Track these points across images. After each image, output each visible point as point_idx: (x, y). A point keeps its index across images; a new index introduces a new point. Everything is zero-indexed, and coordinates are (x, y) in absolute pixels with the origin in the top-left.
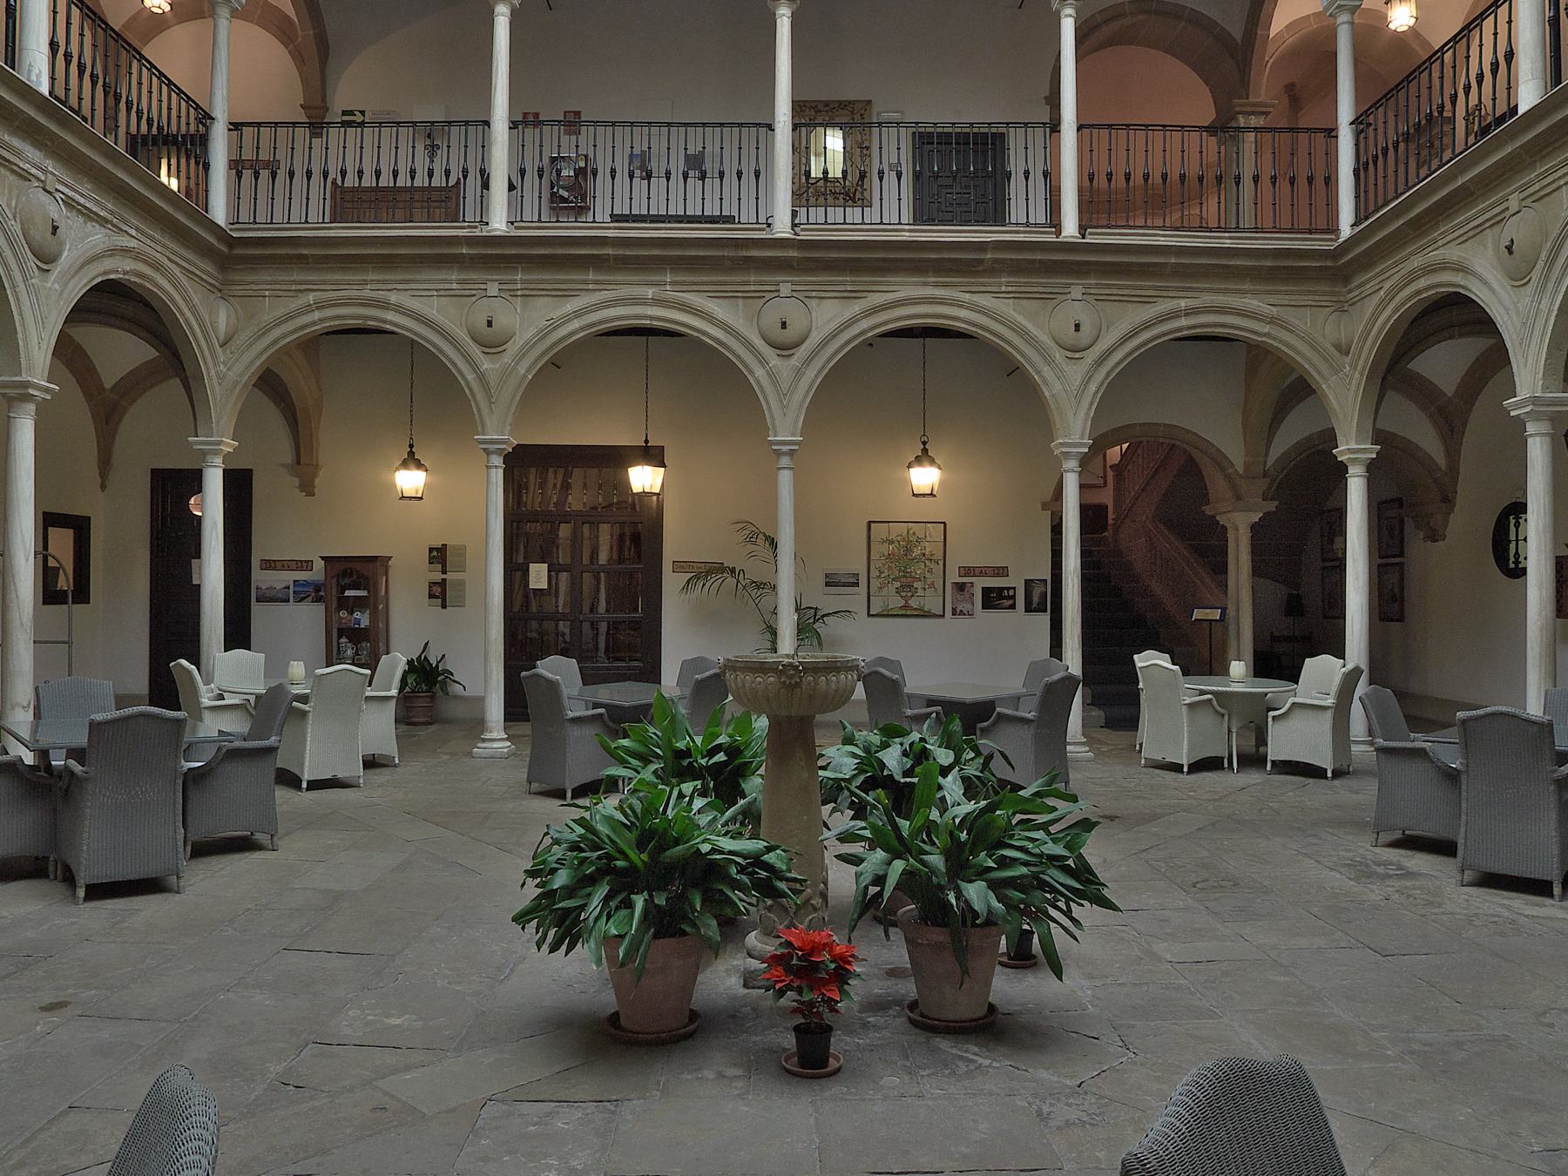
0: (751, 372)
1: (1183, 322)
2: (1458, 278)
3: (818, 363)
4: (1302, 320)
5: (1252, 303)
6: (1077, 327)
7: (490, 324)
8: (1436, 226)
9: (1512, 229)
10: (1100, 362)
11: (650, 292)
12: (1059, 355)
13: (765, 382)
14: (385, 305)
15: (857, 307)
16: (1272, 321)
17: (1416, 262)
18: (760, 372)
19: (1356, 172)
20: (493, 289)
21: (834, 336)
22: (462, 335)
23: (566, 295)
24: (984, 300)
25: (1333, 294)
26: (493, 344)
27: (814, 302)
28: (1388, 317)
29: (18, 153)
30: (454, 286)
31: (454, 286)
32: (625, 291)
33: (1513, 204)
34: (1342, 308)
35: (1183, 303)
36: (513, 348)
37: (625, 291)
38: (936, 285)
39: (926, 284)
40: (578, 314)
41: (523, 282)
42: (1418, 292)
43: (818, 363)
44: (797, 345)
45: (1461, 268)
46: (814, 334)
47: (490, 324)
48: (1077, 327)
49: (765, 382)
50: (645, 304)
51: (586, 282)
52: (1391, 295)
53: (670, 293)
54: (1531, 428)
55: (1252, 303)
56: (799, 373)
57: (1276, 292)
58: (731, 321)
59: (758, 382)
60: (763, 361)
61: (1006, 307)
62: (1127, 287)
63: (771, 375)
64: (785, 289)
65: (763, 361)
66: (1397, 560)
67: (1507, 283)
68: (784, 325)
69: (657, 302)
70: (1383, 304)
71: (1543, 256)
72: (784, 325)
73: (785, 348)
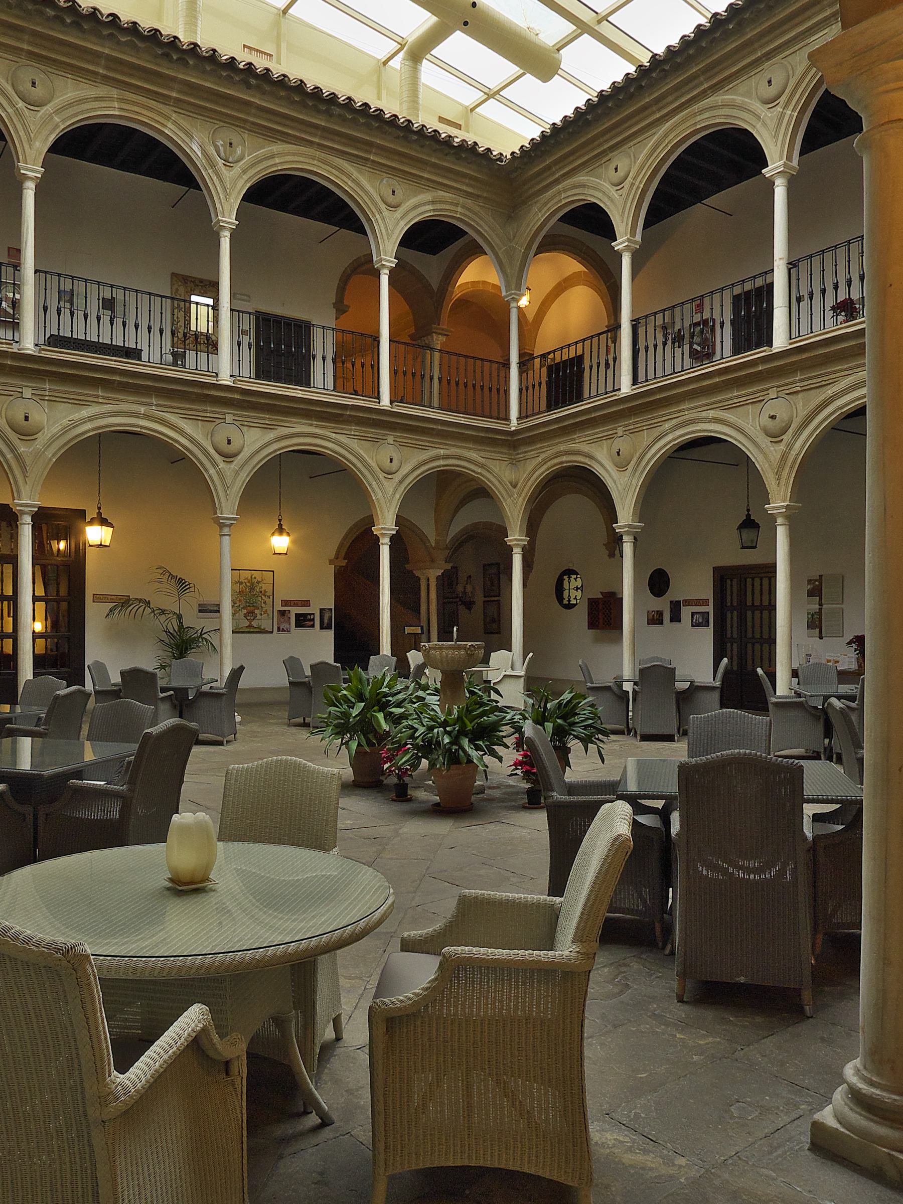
0: (207, 470)
1: (442, 462)
2: (587, 460)
3: (248, 468)
4: (495, 467)
5: (473, 455)
6: (391, 460)
7: (27, 419)
8: (574, 432)
9: (618, 444)
10: (401, 482)
11: (142, 410)
12: (381, 475)
13: (216, 478)
15: (272, 435)
16: (482, 466)
17: (562, 447)
18: (212, 471)
19: (520, 390)
20: (27, 393)
21: (258, 452)
23: (82, 404)
24: (343, 439)
25: (510, 454)
26: (27, 433)
27: (245, 429)
28: (542, 472)
32: (124, 407)
33: (620, 431)
34: (514, 463)
35: (442, 452)
37: (124, 407)
38: (317, 426)
39: (311, 425)
40: (90, 419)
41: (50, 390)
42: (562, 463)
43: (248, 468)
45: (592, 457)
46: (246, 449)
47: (27, 419)
48: (391, 460)
49: (216, 478)
52: (545, 461)
53: (154, 411)
54: (625, 538)
55: (473, 455)
56: (237, 473)
57: (485, 451)
58: (195, 435)
59: (210, 477)
60: (215, 464)
61: (354, 444)
62: (416, 440)
63: (220, 473)
64: (229, 418)
65: (215, 464)
66: (488, 599)
67: (615, 468)
68: (229, 442)
69: (147, 417)
70: (541, 465)
71: (635, 459)
72: (229, 442)
73: (229, 457)
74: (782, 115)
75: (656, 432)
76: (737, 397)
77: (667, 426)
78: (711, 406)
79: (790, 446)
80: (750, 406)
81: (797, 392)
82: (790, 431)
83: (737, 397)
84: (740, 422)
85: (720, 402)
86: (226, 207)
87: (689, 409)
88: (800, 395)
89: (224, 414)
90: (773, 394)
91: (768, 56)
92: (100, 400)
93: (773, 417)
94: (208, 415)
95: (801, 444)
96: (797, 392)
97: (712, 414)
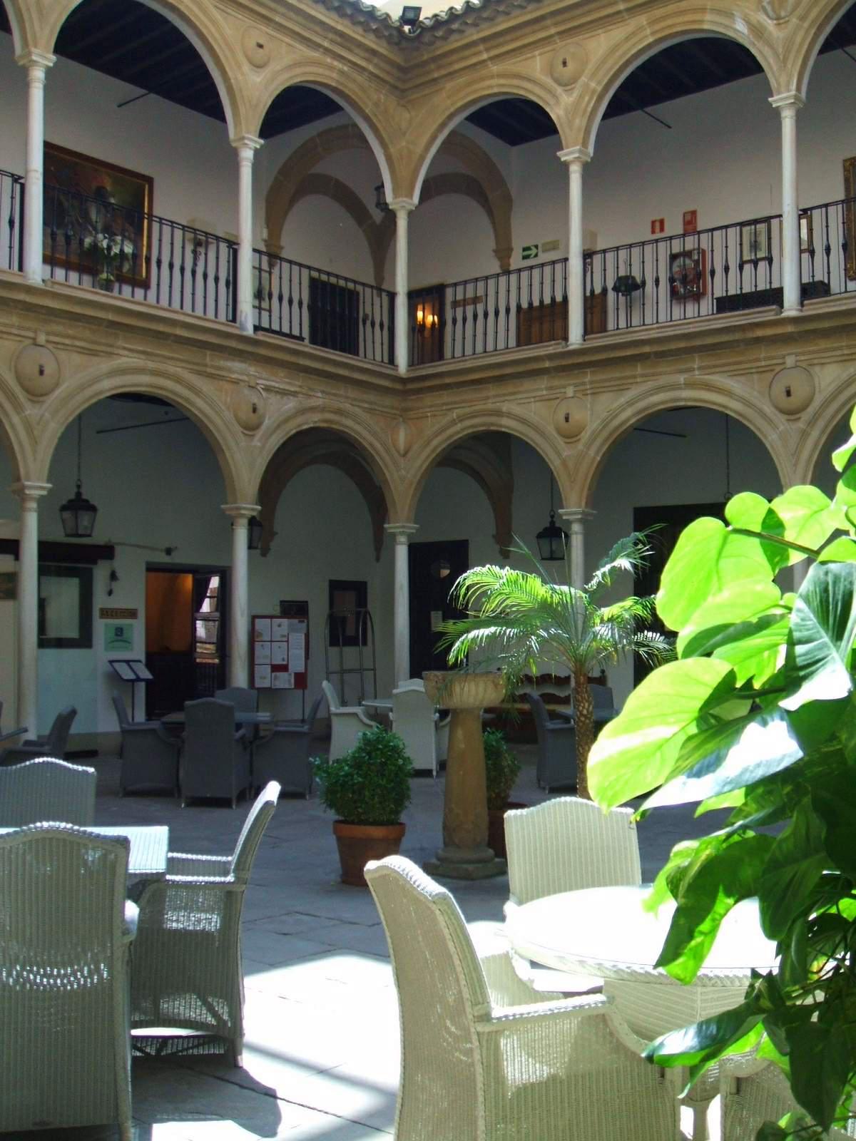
3: (821, 423)
11: (682, 378)
14: (499, 413)
20: (570, 391)
22: (551, 430)
23: (622, 389)
26: (571, 436)
27: (817, 369)
29: (230, 370)
30: (545, 392)
31: (545, 392)
32: (663, 380)
36: (585, 436)
37: (663, 380)
40: (630, 403)
41: (591, 382)
43: (821, 423)
44: (803, 408)
47: (567, 419)
50: (680, 389)
51: (635, 377)
53: (698, 375)
56: (804, 435)
64: (790, 361)
68: (788, 393)
69: (690, 385)
72: (788, 393)
86: (783, 80)
89: (784, 357)
92: (638, 380)
94: (763, 363)
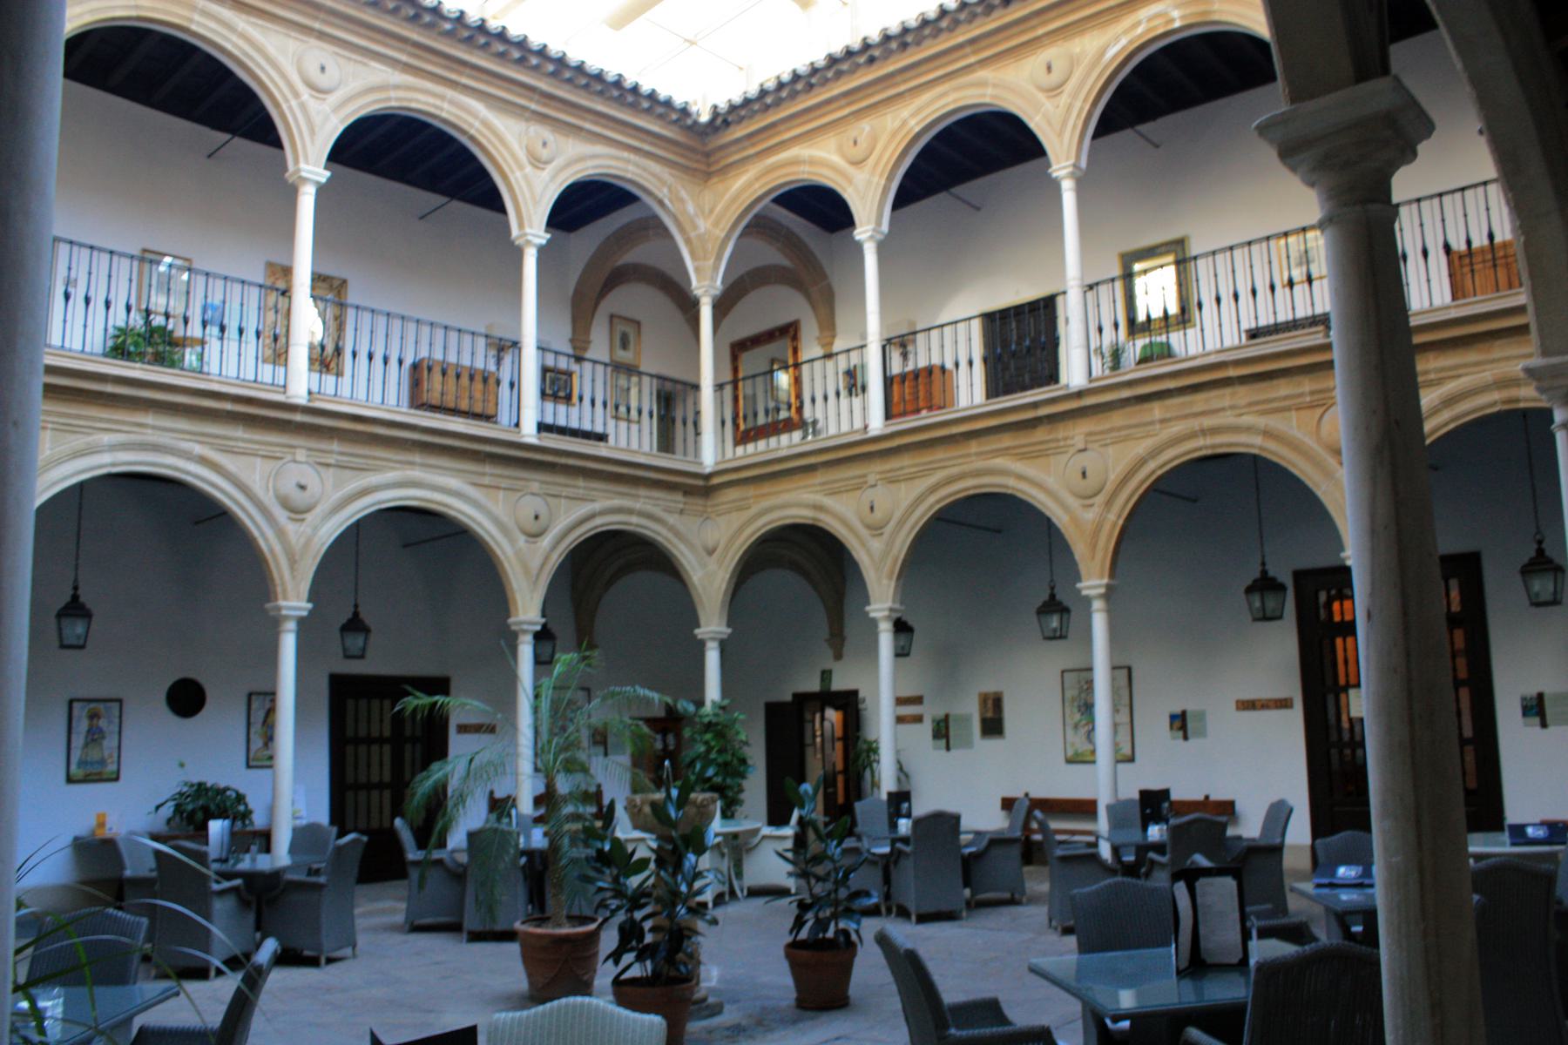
74: (326, 119)
75: (79, 441)
76: (244, 440)
77: (107, 438)
78: (201, 438)
79: (316, 529)
80: (259, 460)
81: (328, 465)
82: (318, 510)
83: (244, 440)
84: (244, 477)
85: (217, 437)
87: (154, 427)
88: (331, 470)
90: (301, 455)
91: (322, 36)
93: (303, 487)
95: (329, 530)
96: (328, 465)
97: (198, 449)
